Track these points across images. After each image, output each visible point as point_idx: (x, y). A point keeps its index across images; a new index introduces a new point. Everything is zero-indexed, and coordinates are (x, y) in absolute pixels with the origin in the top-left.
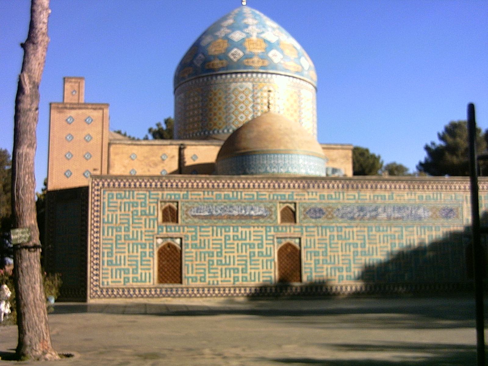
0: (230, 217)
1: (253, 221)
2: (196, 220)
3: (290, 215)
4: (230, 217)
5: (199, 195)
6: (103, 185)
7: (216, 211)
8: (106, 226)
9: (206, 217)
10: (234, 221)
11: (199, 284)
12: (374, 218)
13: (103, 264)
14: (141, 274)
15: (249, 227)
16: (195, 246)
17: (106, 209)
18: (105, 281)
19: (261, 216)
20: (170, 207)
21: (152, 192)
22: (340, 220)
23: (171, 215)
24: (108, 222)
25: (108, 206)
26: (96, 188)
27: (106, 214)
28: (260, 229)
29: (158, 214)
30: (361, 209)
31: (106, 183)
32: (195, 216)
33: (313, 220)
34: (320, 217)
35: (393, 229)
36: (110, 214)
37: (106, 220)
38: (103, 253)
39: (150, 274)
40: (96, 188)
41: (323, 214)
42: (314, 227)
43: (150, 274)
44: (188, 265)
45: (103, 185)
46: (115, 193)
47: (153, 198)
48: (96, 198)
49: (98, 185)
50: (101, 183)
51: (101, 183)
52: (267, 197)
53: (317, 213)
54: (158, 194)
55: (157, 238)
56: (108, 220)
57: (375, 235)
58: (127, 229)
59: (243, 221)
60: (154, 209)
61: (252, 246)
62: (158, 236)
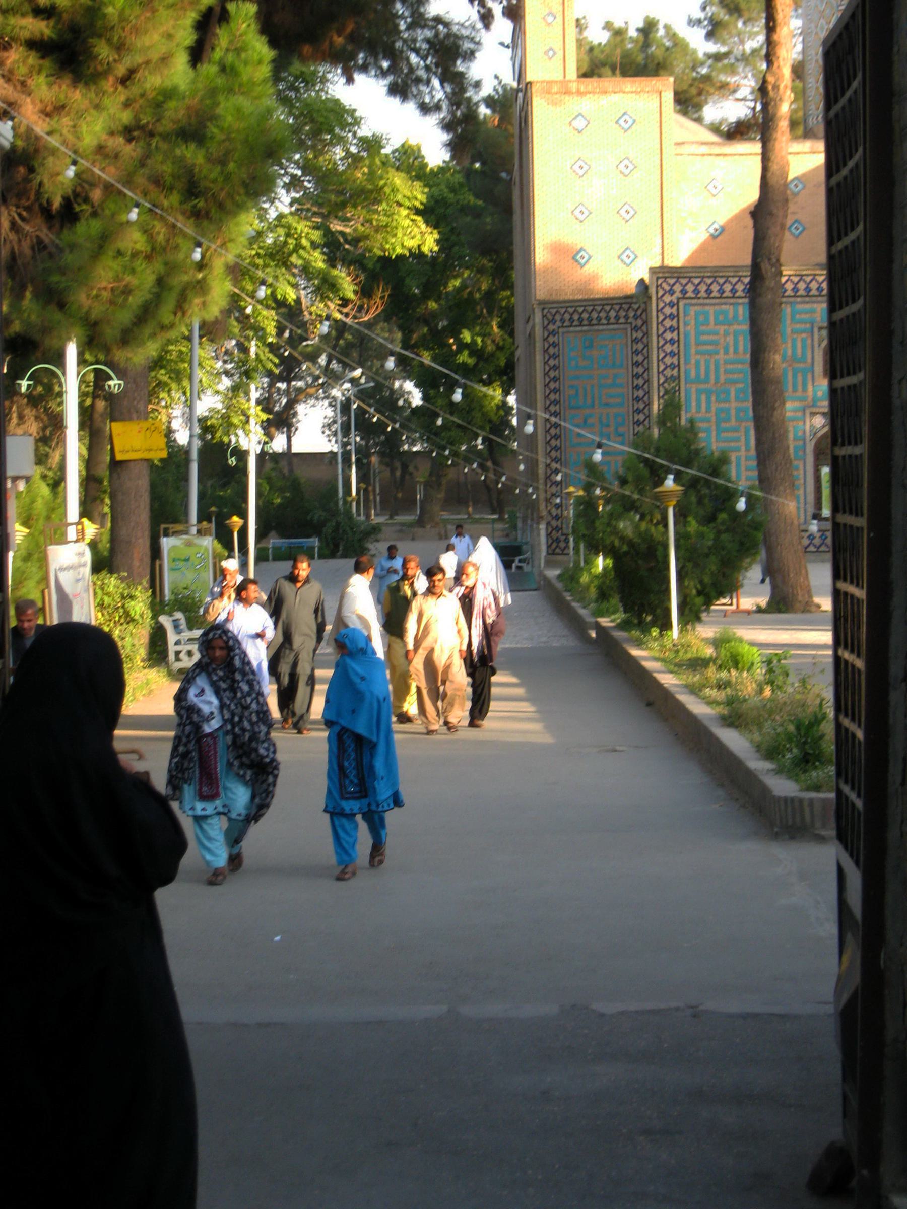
6: (684, 292)
17: (693, 351)
21: (800, 307)
24: (698, 381)
25: (697, 344)
26: (667, 299)
27: (693, 361)
29: (813, 358)
31: (690, 288)
37: (693, 374)
40: (667, 299)
45: (684, 292)
46: (711, 310)
47: (801, 322)
48: (668, 323)
49: (672, 292)
50: (678, 288)
51: (678, 288)
54: (813, 312)
55: (813, 414)
56: (698, 375)
60: (803, 347)
62: (814, 410)
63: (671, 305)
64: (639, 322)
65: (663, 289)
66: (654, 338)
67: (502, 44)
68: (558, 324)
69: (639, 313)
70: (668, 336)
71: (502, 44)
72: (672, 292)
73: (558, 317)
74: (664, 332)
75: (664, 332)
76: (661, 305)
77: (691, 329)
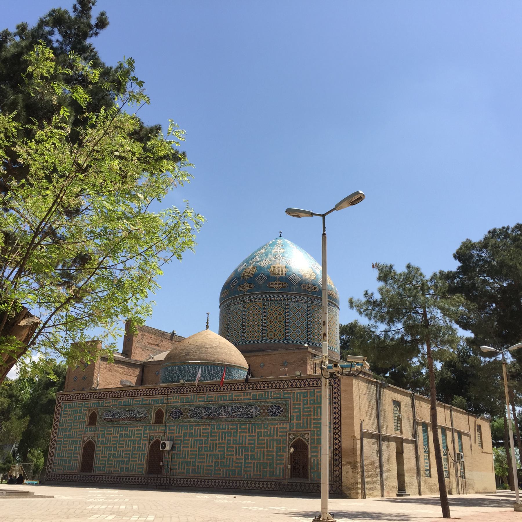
0: (124, 419)
2: (105, 422)
3: (159, 418)
4: (124, 419)
5: (110, 402)
8: (60, 427)
9: (111, 420)
12: (216, 417)
13: (55, 456)
15: (134, 427)
16: (103, 443)
19: (142, 418)
20: (94, 413)
22: (192, 420)
23: (93, 419)
28: (141, 428)
30: (208, 410)
33: (174, 420)
35: (230, 427)
42: (174, 426)
52: (148, 402)
53: (177, 413)
57: (216, 432)
61: (134, 442)
72: (60, 399)
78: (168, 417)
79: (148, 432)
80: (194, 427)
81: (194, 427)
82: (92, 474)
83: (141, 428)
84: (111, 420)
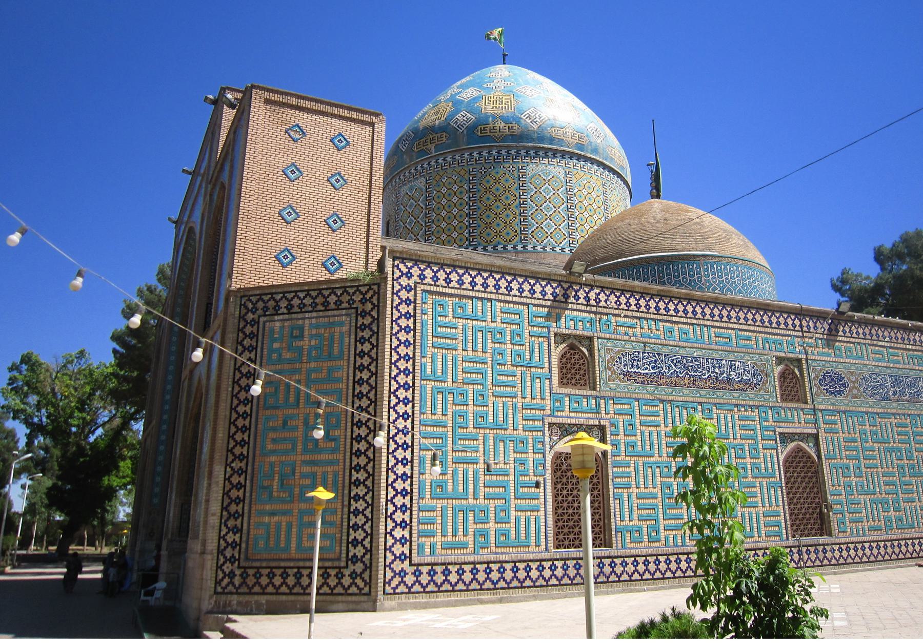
1: (736, 395)
2: (632, 386)
7: (669, 367)
10: (703, 392)
11: (645, 547)
14: (517, 520)
18: (427, 542)
26: (404, 281)
30: (896, 381)
32: (627, 374)
34: (840, 393)
36: (439, 353)
38: (422, 461)
39: (537, 520)
41: (844, 385)
43: (537, 520)
44: (619, 498)
49: (409, 276)
58: (481, 399)
59: (720, 394)
63: (408, 289)
64: (369, 306)
65: (400, 271)
66: (388, 323)
67: (170, 219)
68: (260, 312)
69: (368, 296)
70: (403, 322)
71: (170, 219)
73: (260, 305)
74: (399, 318)
75: (399, 318)
76: (397, 287)
77: (428, 318)
78: (815, 389)
79: (771, 423)
80: (878, 419)
81: (878, 419)
82: (613, 552)
83: (749, 413)
84: (648, 380)
